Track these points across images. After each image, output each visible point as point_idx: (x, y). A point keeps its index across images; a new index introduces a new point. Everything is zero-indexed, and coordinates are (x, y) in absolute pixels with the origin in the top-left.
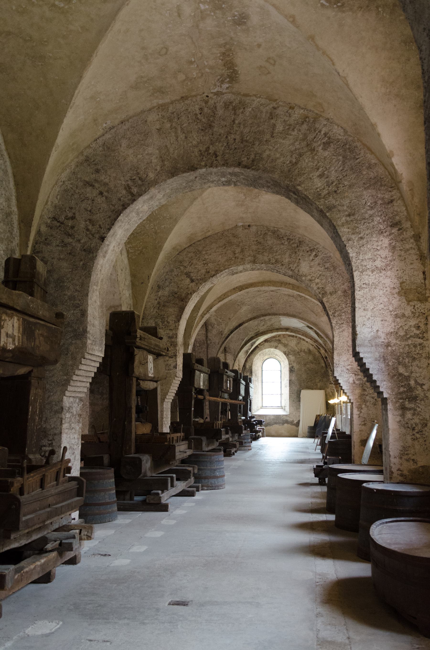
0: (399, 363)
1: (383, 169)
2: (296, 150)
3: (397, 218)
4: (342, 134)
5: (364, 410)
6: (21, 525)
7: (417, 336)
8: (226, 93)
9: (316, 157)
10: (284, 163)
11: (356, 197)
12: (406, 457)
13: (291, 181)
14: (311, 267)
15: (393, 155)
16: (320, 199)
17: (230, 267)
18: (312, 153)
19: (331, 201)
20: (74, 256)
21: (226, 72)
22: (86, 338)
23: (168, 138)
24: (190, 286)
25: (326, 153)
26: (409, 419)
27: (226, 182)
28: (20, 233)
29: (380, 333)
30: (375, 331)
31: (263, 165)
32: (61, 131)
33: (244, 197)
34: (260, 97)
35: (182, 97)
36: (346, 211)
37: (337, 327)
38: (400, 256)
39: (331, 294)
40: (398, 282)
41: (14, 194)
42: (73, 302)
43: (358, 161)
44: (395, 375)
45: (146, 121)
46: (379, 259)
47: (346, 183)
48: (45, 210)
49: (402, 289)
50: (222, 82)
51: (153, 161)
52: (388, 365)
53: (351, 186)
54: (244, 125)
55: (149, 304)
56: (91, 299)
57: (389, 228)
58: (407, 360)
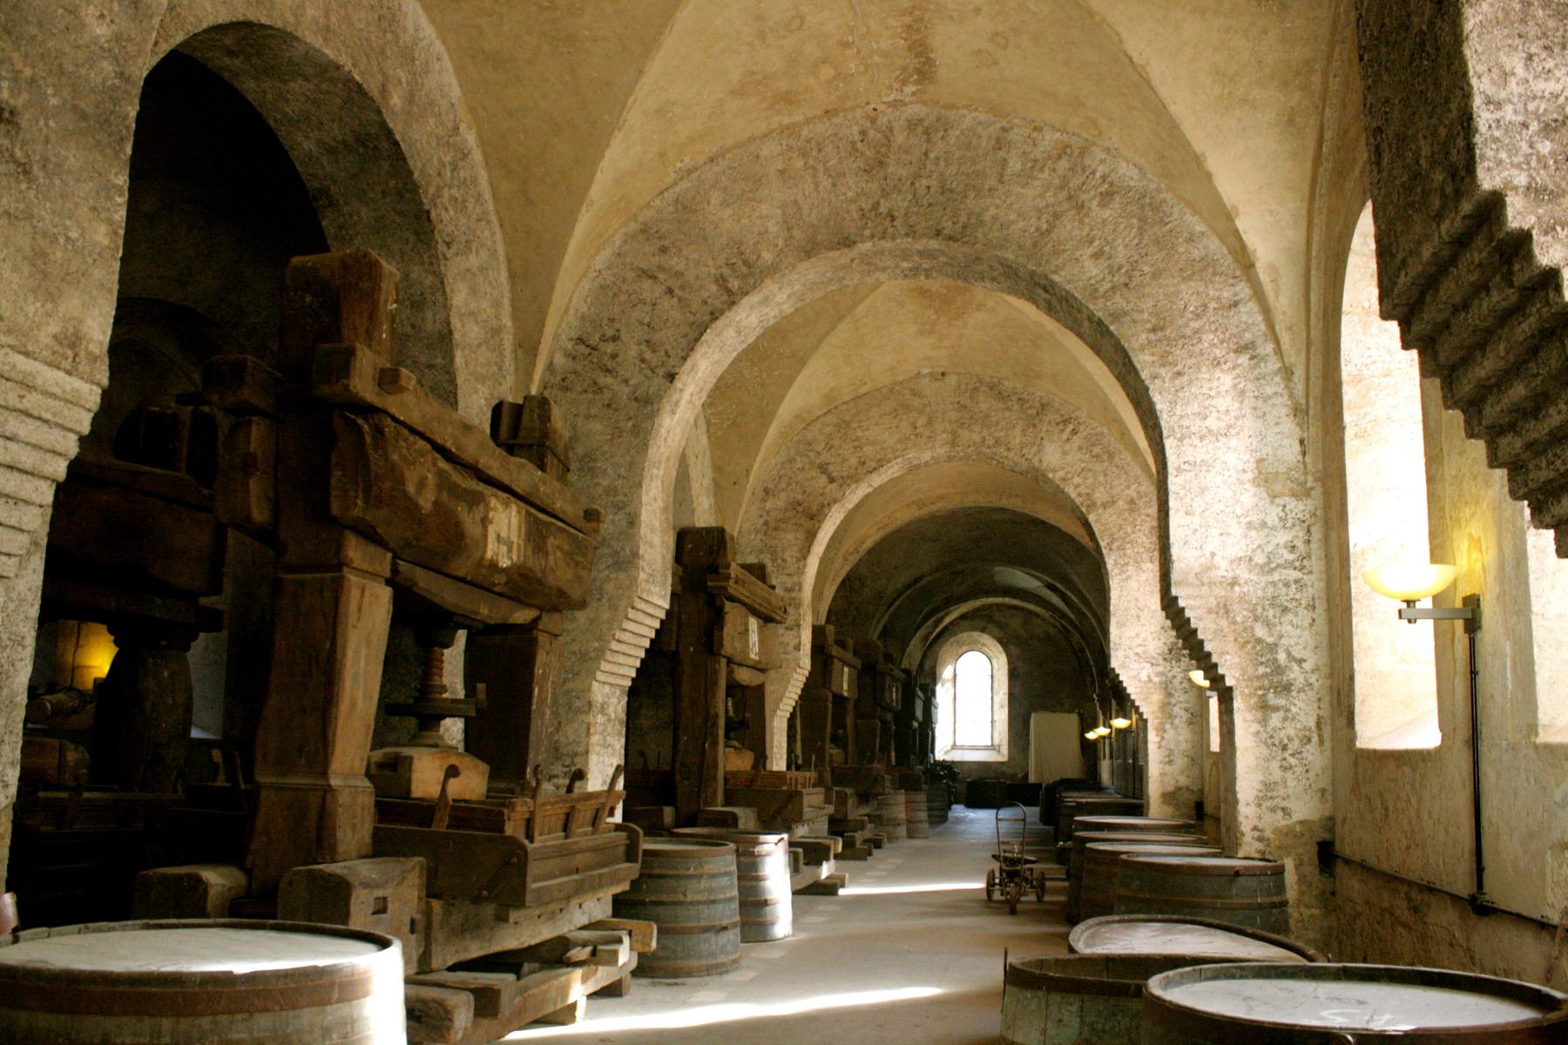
0: (1256, 619)
1: (1217, 242)
2: (1047, 206)
3: (1248, 336)
4: (1136, 177)
5: (1170, 734)
6: (529, 897)
7: (1289, 565)
8: (911, 103)
9: (1087, 221)
10: (1025, 231)
11: (1166, 295)
12: (1269, 803)
13: (1040, 265)
14: (1065, 453)
15: (1237, 215)
16: (1096, 298)
18: (1079, 213)
19: (1118, 301)
20: (616, 410)
21: (912, 63)
22: (637, 568)
23: (800, 187)
24: (827, 490)
25: (1107, 213)
26: (1274, 730)
27: (911, 270)
28: (516, 370)
29: (1217, 560)
30: (1208, 555)
31: (985, 235)
32: (599, 173)
33: (934, 317)
34: (976, 110)
35: (827, 112)
36: (1148, 321)
37: (1117, 571)
38: (1255, 409)
39: (1104, 506)
40: (1252, 460)
41: (507, 295)
42: (611, 498)
43: (1168, 227)
44: (1248, 642)
45: (757, 157)
46: (1214, 415)
47: (1146, 269)
48: (564, 324)
49: (1260, 473)
50: (904, 82)
51: (770, 229)
52: (1235, 622)
53: (1156, 275)
54: (945, 161)
55: (748, 524)
56: (647, 494)
57: (1232, 355)
58: (1271, 613)
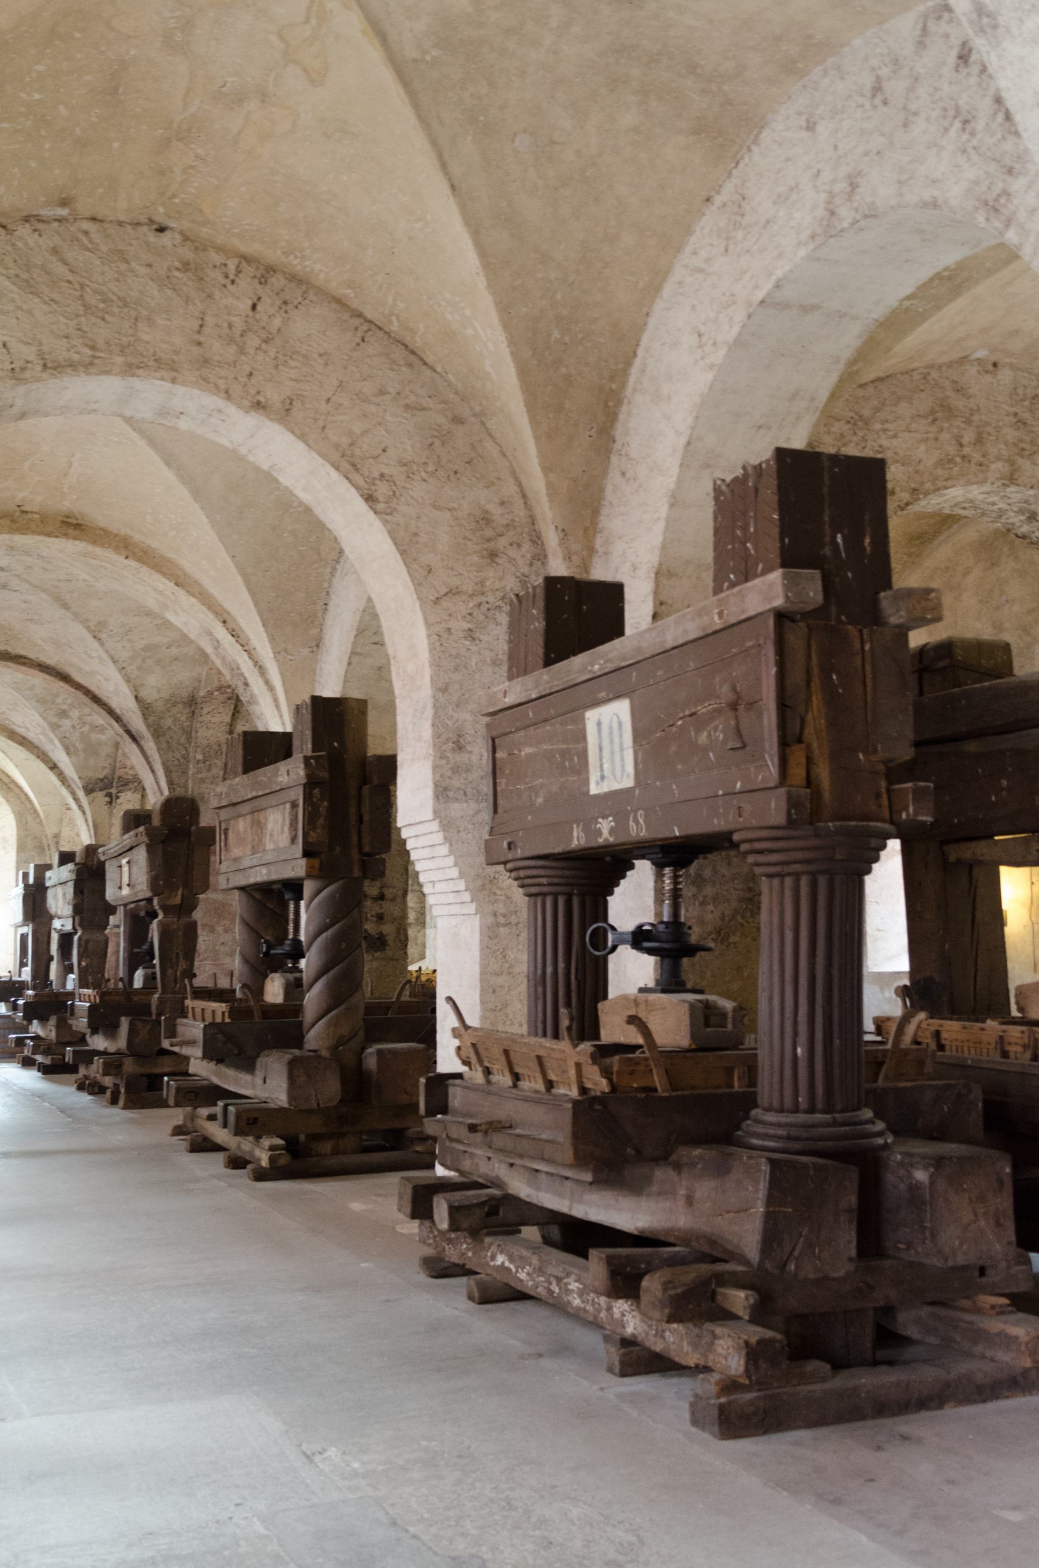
17: (949, 483)
